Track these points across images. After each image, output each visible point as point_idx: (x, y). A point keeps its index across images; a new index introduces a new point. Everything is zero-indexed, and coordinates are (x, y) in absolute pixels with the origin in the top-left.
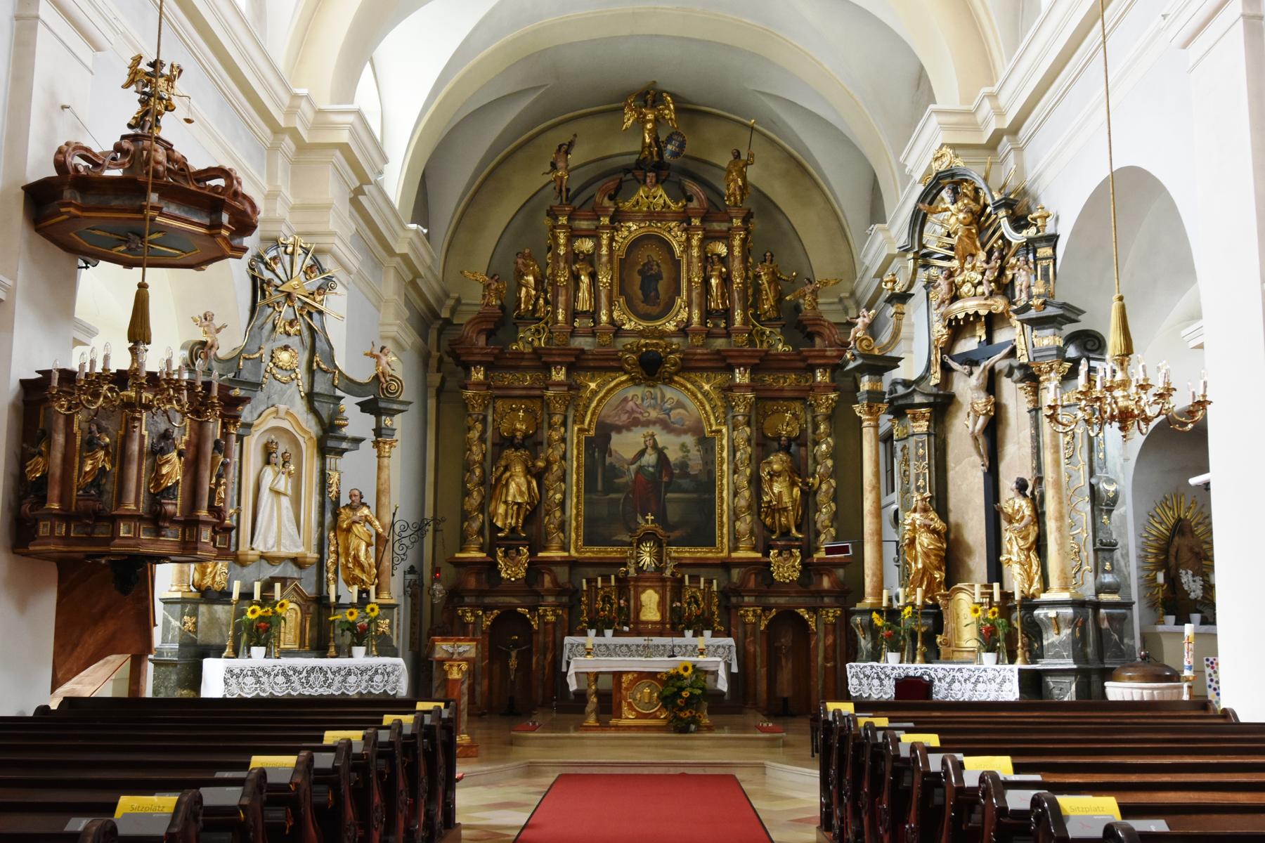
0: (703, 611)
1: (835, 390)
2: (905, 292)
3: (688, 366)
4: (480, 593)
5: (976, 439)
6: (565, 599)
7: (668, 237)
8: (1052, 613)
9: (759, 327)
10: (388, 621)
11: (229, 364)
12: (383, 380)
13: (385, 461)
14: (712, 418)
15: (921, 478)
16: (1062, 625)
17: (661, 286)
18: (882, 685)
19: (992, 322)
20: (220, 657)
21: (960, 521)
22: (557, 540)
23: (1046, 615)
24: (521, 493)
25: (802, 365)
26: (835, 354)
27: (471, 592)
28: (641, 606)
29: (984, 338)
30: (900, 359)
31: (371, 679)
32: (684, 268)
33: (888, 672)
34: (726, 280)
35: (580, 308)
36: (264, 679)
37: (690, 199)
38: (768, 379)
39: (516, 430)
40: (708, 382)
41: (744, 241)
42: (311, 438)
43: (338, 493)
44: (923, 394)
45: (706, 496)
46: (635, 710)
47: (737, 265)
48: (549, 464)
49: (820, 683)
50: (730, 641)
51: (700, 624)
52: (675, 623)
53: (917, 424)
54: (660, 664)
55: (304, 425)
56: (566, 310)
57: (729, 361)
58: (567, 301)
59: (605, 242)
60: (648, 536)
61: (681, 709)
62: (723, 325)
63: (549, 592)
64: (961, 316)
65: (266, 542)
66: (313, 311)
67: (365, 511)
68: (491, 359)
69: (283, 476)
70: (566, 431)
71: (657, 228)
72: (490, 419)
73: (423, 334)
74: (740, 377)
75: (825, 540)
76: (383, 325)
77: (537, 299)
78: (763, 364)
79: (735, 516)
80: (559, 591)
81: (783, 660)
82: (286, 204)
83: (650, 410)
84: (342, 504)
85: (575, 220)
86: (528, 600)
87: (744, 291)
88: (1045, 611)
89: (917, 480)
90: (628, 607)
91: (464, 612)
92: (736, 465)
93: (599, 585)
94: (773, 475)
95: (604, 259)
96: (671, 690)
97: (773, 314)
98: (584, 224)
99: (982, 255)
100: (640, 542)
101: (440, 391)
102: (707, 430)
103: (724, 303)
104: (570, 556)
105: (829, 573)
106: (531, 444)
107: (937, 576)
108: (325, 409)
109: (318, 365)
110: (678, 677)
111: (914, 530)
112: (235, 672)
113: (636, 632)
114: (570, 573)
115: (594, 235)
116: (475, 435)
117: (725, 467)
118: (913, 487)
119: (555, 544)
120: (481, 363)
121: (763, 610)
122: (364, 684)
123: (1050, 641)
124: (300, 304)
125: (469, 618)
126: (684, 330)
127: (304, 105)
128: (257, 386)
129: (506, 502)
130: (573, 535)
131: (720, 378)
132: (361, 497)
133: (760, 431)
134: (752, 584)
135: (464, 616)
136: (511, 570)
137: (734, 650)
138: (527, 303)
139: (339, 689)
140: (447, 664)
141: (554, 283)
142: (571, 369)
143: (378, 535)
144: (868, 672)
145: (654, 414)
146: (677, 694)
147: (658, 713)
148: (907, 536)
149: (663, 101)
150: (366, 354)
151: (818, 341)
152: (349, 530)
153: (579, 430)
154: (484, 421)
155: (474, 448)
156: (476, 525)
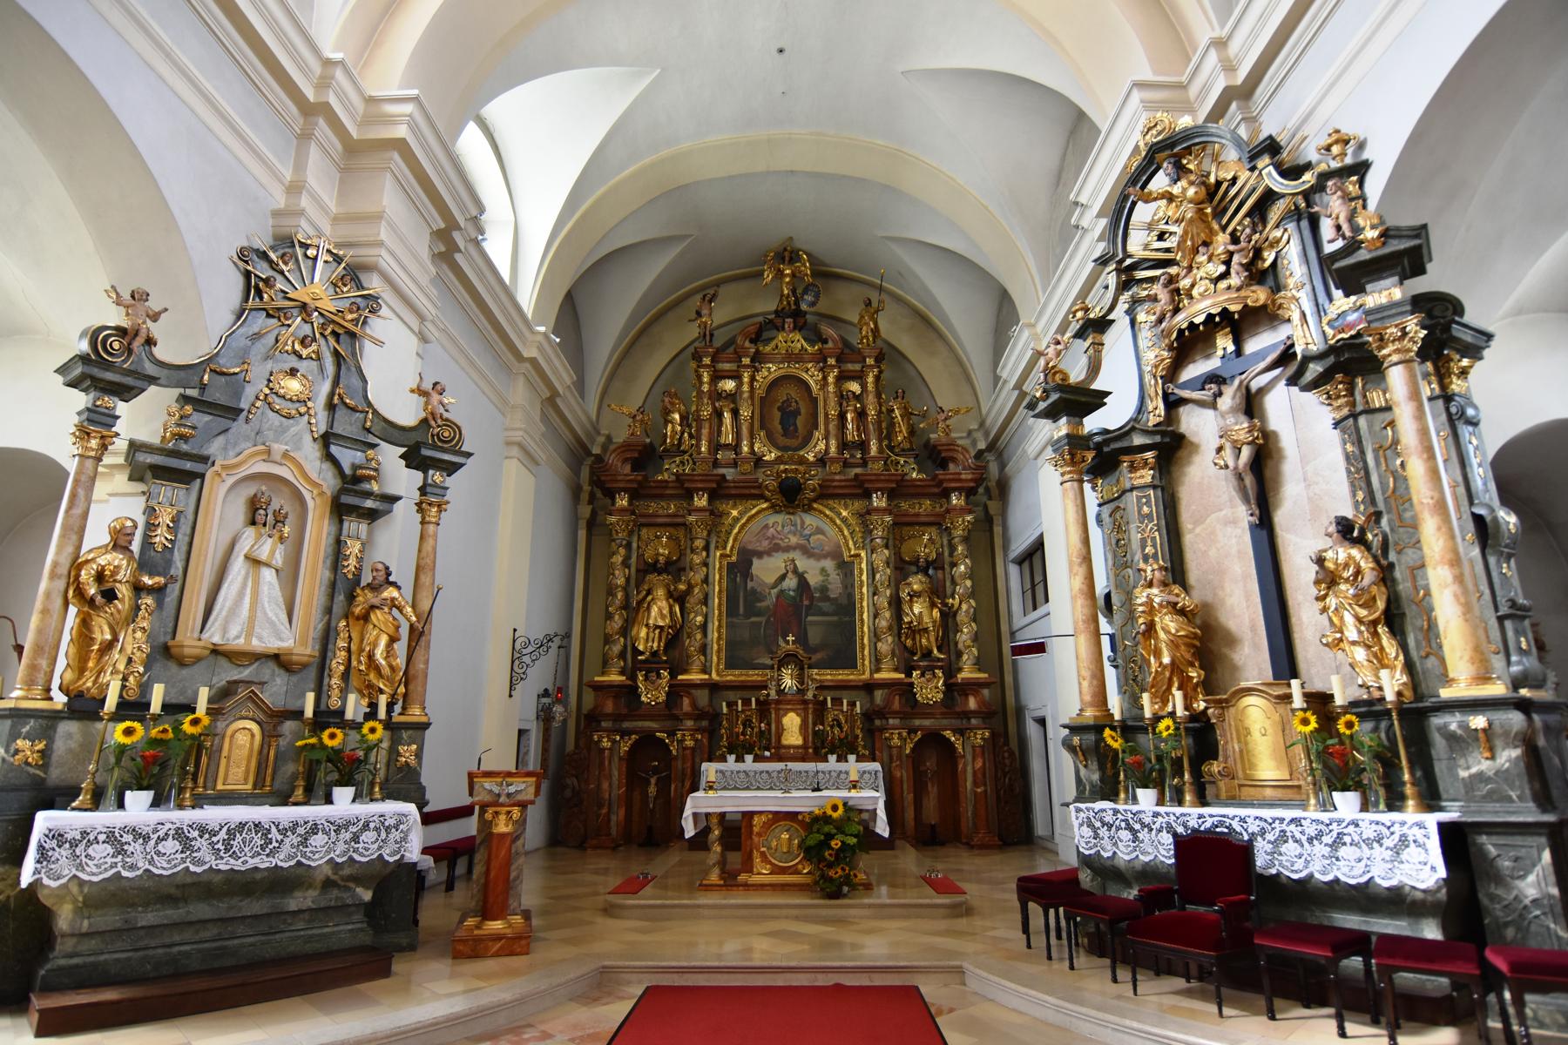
0: (846, 737)
1: (970, 512)
2: (1104, 316)
3: (826, 493)
4: (617, 718)
5: (1240, 477)
6: (705, 723)
7: (805, 376)
8: (1478, 722)
9: (894, 457)
10: (414, 747)
11: (182, 374)
12: (433, 423)
13: (431, 528)
14: (851, 543)
15: (1149, 543)
16: (1498, 743)
17: (800, 421)
18: (1135, 839)
19: (1240, 323)
20: (65, 809)
21: (1209, 599)
22: (697, 662)
23: (1464, 726)
24: (663, 617)
25: (936, 490)
26: (970, 477)
27: (608, 716)
28: (783, 730)
29: (1231, 348)
30: (1107, 394)
31: (355, 838)
32: (821, 404)
33: (1147, 820)
34: (861, 415)
35: (722, 441)
36: (135, 847)
37: (825, 341)
38: (904, 505)
39: (658, 554)
40: (846, 509)
41: (877, 378)
42: (322, 494)
43: (359, 569)
44: (1146, 432)
45: (847, 619)
46: (770, 863)
47: (871, 399)
48: (690, 587)
49: (970, 809)
50: (876, 766)
51: (844, 749)
52: (817, 748)
53: (1138, 474)
54: (801, 800)
55: (314, 476)
56: (710, 442)
57: (866, 485)
58: (711, 433)
59: (746, 380)
60: (788, 659)
61: (830, 866)
62: (859, 456)
63: (689, 716)
64: (1199, 320)
65: (228, 630)
66: (341, 331)
67: (391, 593)
68: (635, 485)
69: (270, 541)
70: (708, 556)
71: (795, 369)
72: (635, 545)
73: (577, 472)
74: (878, 501)
75: (967, 660)
76: (506, 429)
77: (682, 433)
78: (899, 490)
79: (876, 636)
80: (698, 715)
81: (930, 785)
82: (327, 213)
83: (790, 536)
84: (363, 584)
85: (718, 362)
86: (668, 724)
87: (879, 422)
88: (1458, 717)
89: (1143, 548)
90: (770, 730)
91: (601, 738)
92: (876, 587)
93: (740, 709)
94: (914, 595)
95: (746, 395)
96: (817, 838)
97: (906, 445)
98: (727, 366)
99: (1221, 241)
100: (782, 664)
101: (591, 524)
102: (846, 554)
103: (859, 436)
104: (711, 679)
105: (976, 694)
106: (674, 568)
107: (1195, 674)
108: (348, 457)
109: (341, 398)
110: (825, 819)
111: (1150, 608)
112: (69, 836)
113: (780, 759)
114: (711, 700)
115: (737, 377)
116: (618, 559)
117: (865, 590)
118: (1138, 556)
119: (696, 666)
120: (625, 490)
121: (909, 733)
122: (341, 847)
123: (1474, 770)
124: (322, 321)
125: (606, 743)
126: (822, 461)
127: (339, 74)
128: (233, 412)
129: (647, 625)
130: (715, 658)
131: (858, 505)
132: (389, 574)
133: (898, 555)
134: (896, 705)
135: (600, 741)
136: (652, 694)
137: (881, 775)
138: (672, 438)
139: (290, 857)
140: (491, 810)
141: (698, 420)
142: (714, 496)
143: (412, 626)
144: (1109, 818)
145: (794, 540)
146: (825, 844)
147: (800, 867)
148: (1141, 621)
149: (799, 259)
150: (412, 391)
151: (952, 466)
152: (365, 618)
153: (721, 555)
154: (628, 546)
155: (617, 572)
156: (617, 649)
